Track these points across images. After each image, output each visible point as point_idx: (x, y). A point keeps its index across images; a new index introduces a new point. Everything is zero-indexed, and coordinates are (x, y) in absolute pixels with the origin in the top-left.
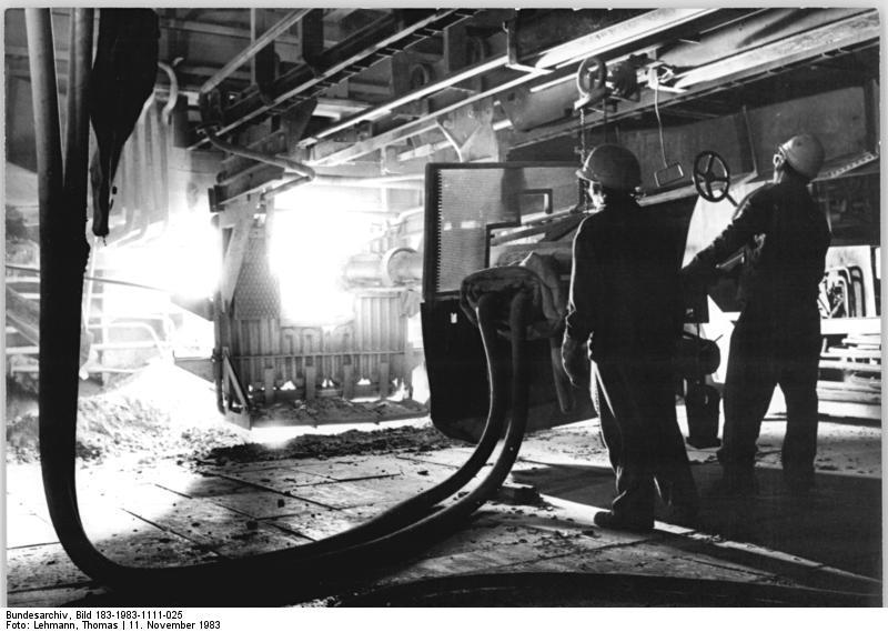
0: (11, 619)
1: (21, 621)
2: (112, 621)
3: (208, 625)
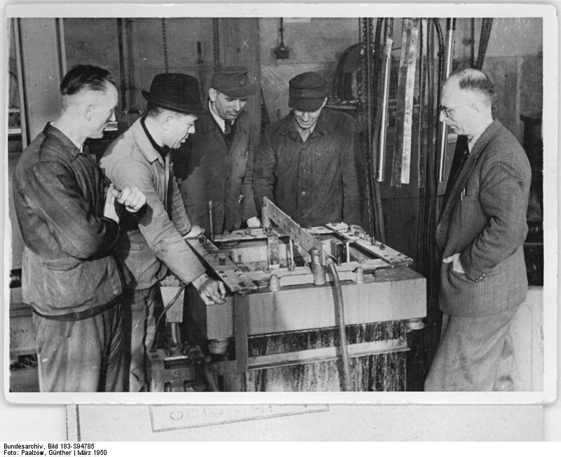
0: (7, 449)
1: (13, 450)
2: (69, 450)
3: (104, 452)
